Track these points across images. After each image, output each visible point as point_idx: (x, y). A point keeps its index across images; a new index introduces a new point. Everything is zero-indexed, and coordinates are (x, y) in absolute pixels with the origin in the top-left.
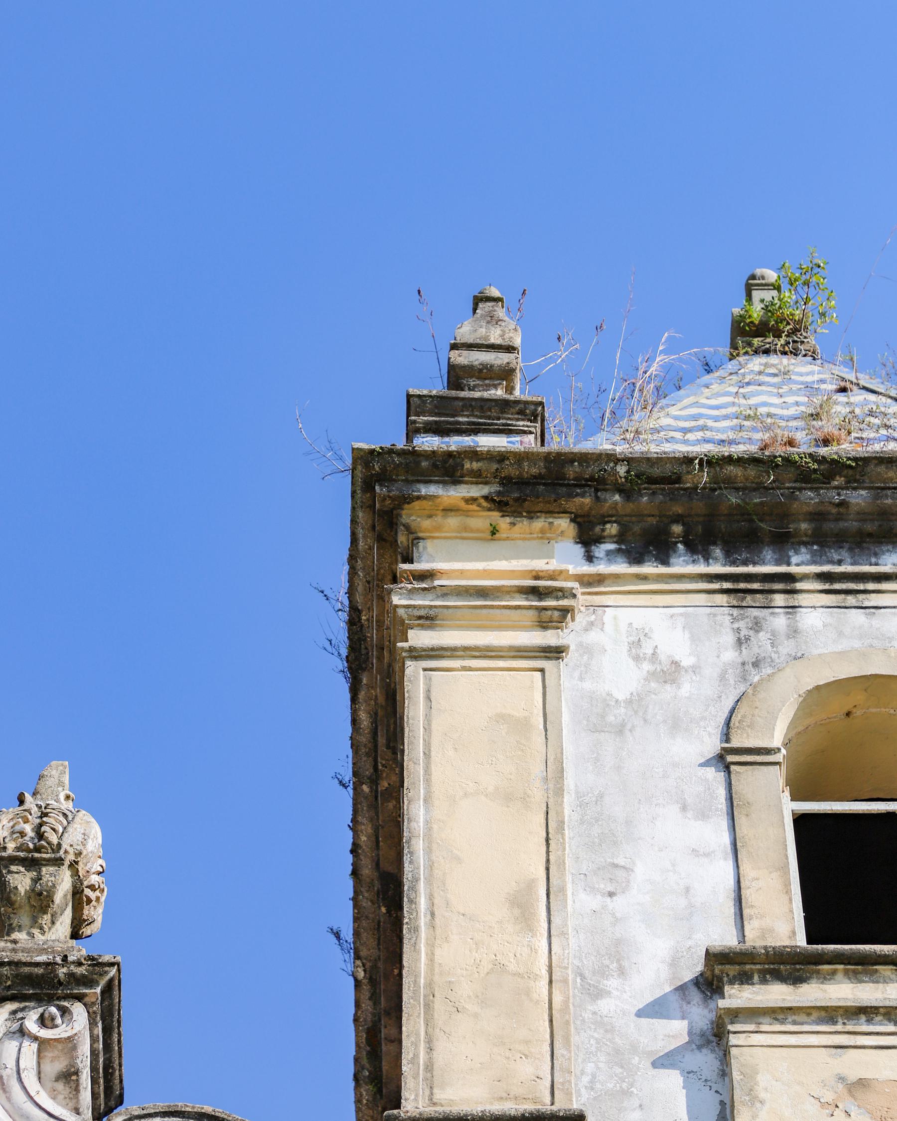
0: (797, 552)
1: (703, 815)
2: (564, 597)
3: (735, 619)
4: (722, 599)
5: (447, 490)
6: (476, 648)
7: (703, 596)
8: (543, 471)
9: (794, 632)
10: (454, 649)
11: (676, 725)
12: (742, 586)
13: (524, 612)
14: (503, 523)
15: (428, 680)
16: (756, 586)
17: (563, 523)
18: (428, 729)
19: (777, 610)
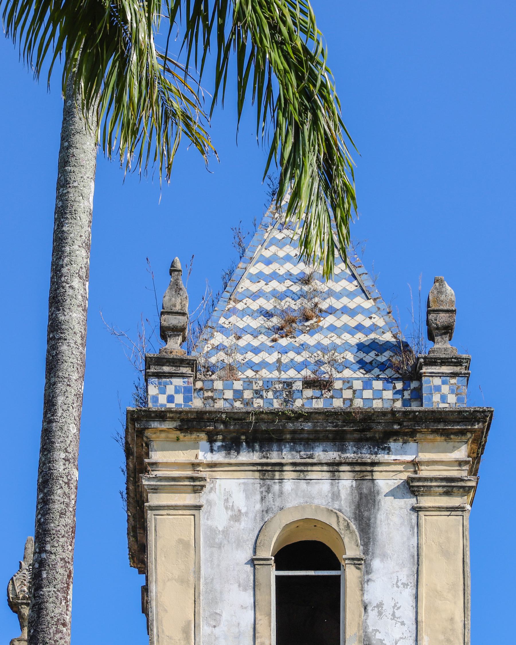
0: (285, 448)
1: (245, 590)
2: (202, 480)
3: (261, 486)
4: (257, 474)
5: (161, 425)
6: (172, 506)
7: (251, 473)
8: (196, 417)
9: (281, 493)
10: (165, 506)
11: (239, 544)
12: (265, 468)
13: (188, 487)
14: (181, 436)
15: (155, 520)
16: (269, 468)
17: (203, 436)
18: (156, 546)
19: (277, 481)
